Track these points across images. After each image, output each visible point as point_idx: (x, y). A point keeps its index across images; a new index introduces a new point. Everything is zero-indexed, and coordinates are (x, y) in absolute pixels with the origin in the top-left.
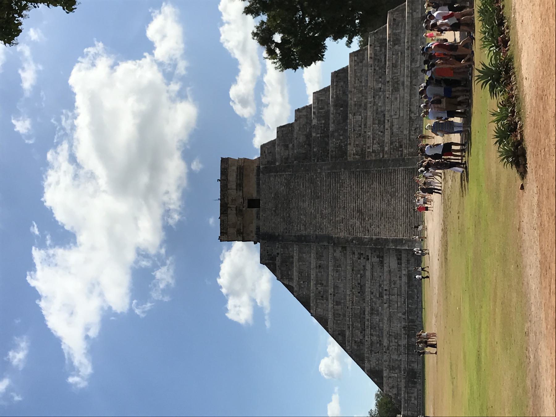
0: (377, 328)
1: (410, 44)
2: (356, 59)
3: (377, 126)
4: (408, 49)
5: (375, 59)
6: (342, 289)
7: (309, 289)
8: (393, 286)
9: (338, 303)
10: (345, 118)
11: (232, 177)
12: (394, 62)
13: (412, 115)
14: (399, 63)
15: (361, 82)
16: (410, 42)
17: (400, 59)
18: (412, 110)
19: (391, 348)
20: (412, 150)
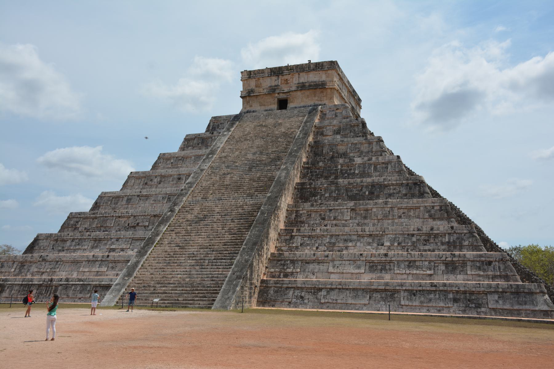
0: (77, 247)
1: (441, 288)
2: (435, 208)
3: (328, 240)
4: (432, 285)
5: (429, 235)
6: (143, 205)
7: (164, 168)
8: (110, 265)
9: (129, 200)
10: (352, 198)
11: (313, 77)
12: (417, 263)
13: (324, 293)
14: (415, 272)
15: (400, 217)
16: (445, 288)
17: (422, 272)
18: (332, 293)
19: (43, 263)
20: (272, 292)
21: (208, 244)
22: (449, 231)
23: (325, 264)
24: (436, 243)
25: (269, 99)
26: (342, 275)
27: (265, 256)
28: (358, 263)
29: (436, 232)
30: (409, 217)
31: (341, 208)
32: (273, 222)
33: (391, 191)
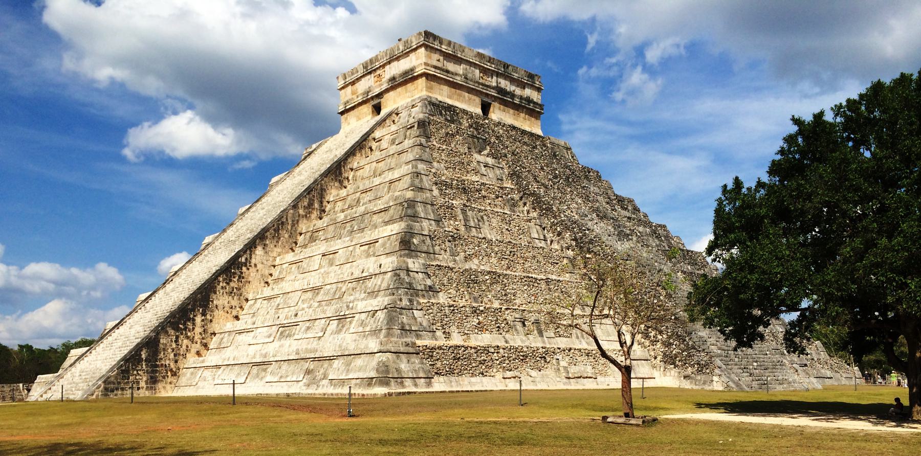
5: (358, 280)
25: (367, 109)
27: (198, 330)
29: (364, 275)
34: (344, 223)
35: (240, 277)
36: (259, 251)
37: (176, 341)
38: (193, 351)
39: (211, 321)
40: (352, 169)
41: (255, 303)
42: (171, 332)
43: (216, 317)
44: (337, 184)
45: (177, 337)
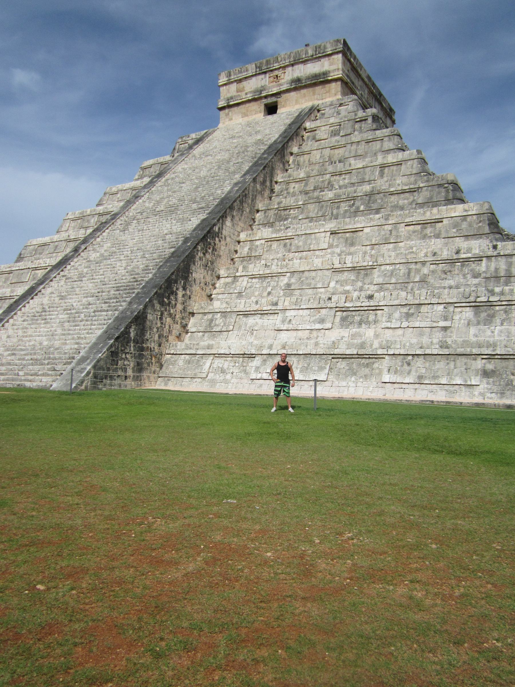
1: (460, 350)
2: (469, 219)
5: (452, 262)
13: (257, 362)
14: (417, 324)
15: (409, 238)
21: (96, 291)
22: (490, 253)
23: (271, 317)
24: (464, 275)
25: (254, 106)
26: (294, 333)
27: (180, 307)
28: (323, 311)
29: (464, 256)
30: (424, 237)
31: (317, 231)
32: (200, 254)
33: (401, 203)
34: (336, 202)
35: (213, 250)
36: (228, 223)
37: (161, 319)
38: (175, 332)
39: (190, 298)
40: (292, 154)
41: (233, 282)
42: (158, 306)
43: (194, 294)
44: (281, 166)
45: (162, 314)
